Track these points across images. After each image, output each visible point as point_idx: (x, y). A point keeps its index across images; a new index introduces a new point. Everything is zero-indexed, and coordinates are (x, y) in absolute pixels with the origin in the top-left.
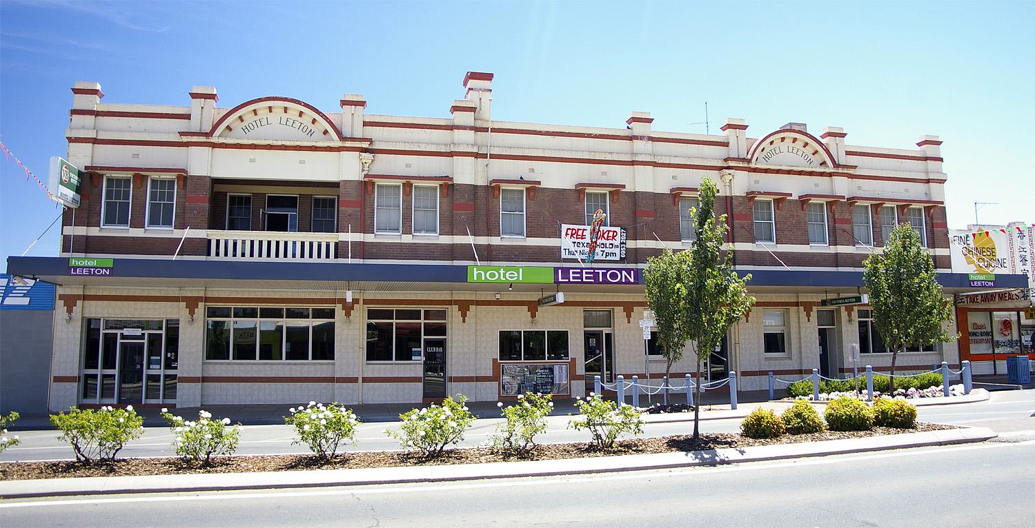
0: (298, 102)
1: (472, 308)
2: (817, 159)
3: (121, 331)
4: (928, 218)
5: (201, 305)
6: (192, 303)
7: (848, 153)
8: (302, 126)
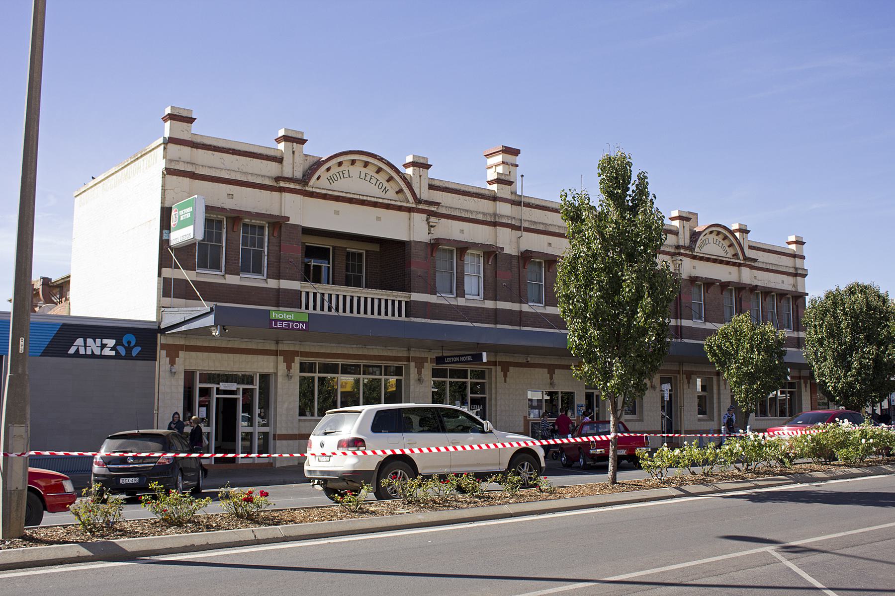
0: (381, 159)
1: (511, 369)
2: (731, 252)
3: (218, 386)
4: (794, 306)
5: (297, 360)
6: (289, 357)
8: (378, 182)
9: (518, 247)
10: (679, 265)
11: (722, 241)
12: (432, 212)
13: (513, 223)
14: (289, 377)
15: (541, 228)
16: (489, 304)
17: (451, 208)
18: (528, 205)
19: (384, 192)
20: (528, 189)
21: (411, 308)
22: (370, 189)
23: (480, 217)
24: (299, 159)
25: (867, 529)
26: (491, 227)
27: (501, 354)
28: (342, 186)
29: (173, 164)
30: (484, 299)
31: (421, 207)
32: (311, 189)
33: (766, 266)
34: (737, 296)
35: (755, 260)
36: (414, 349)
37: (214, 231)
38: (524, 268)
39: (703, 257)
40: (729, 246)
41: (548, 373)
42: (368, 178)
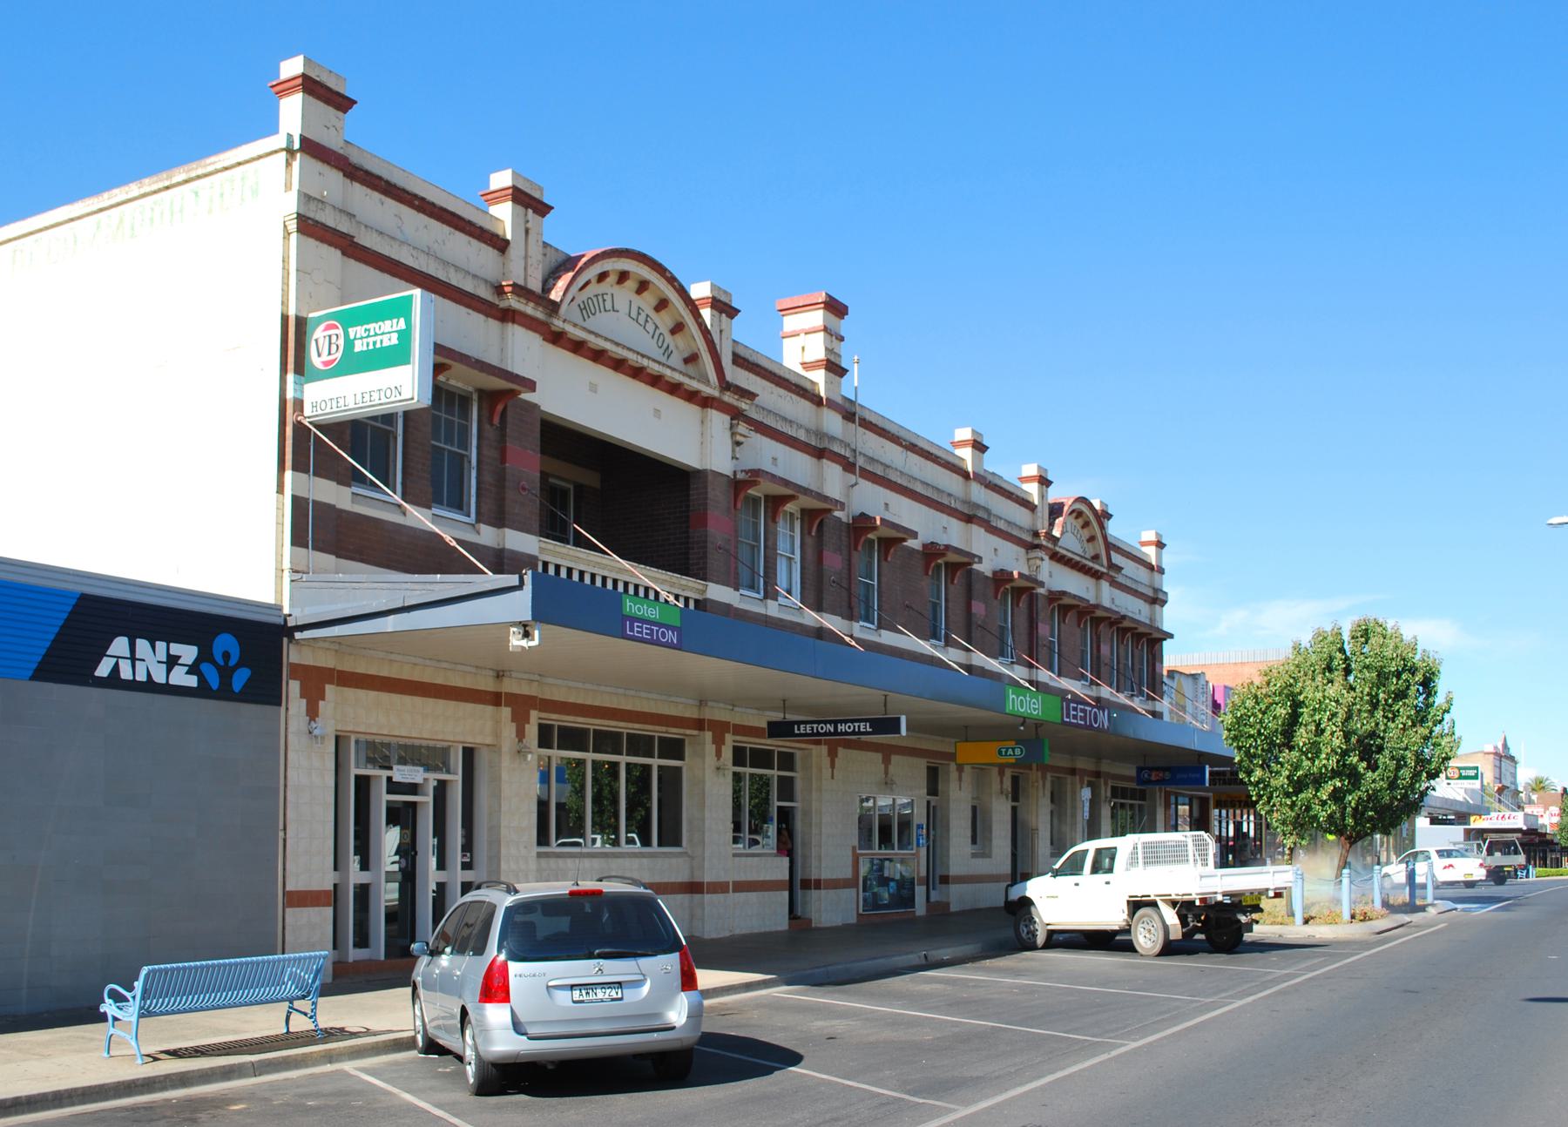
3: (389, 773)
4: (1150, 656)
5: (535, 716)
14: (521, 753)
15: (879, 471)
19: (666, 354)
29: (313, 206)
31: (728, 398)
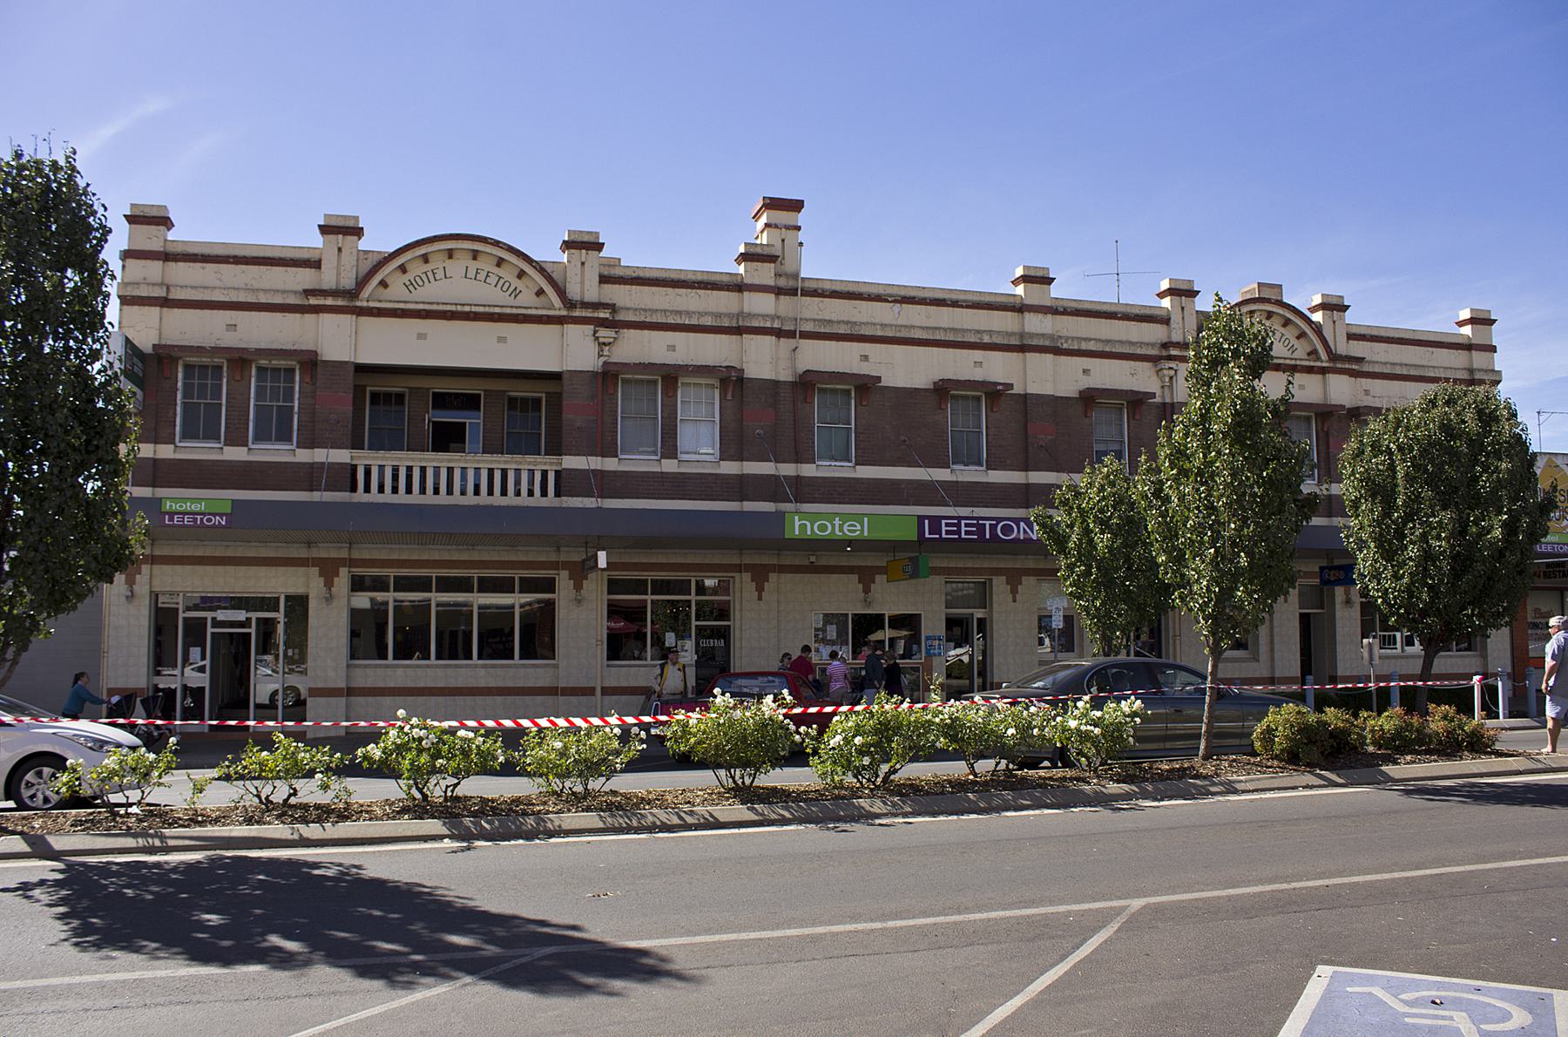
0: (497, 243)
1: (773, 577)
5: (344, 571)
6: (328, 569)
7: (1351, 337)
8: (502, 282)
9: (794, 367)
10: (1171, 378)
11: (1282, 330)
12: (608, 320)
13: (776, 326)
14: (329, 599)
15: (842, 330)
16: (730, 468)
17: (645, 310)
18: (814, 293)
19: (513, 295)
20: (813, 267)
21: (566, 483)
22: (488, 294)
23: (708, 321)
24: (348, 260)
25: (941, 919)
26: (734, 337)
27: (748, 551)
28: (434, 292)
29: (130, 288)
30: (721, 460)
31: (577, 313)
32: (365, 304)
33: (815, 326)
34: (1319, 428)
35: (1360, 360)
36: (565, 549)
37: (269, 384)
38: (1086, 416)
39: (1313, 367)
40: (1298, 338)
41: (860, 582)
42: (482, 276)
